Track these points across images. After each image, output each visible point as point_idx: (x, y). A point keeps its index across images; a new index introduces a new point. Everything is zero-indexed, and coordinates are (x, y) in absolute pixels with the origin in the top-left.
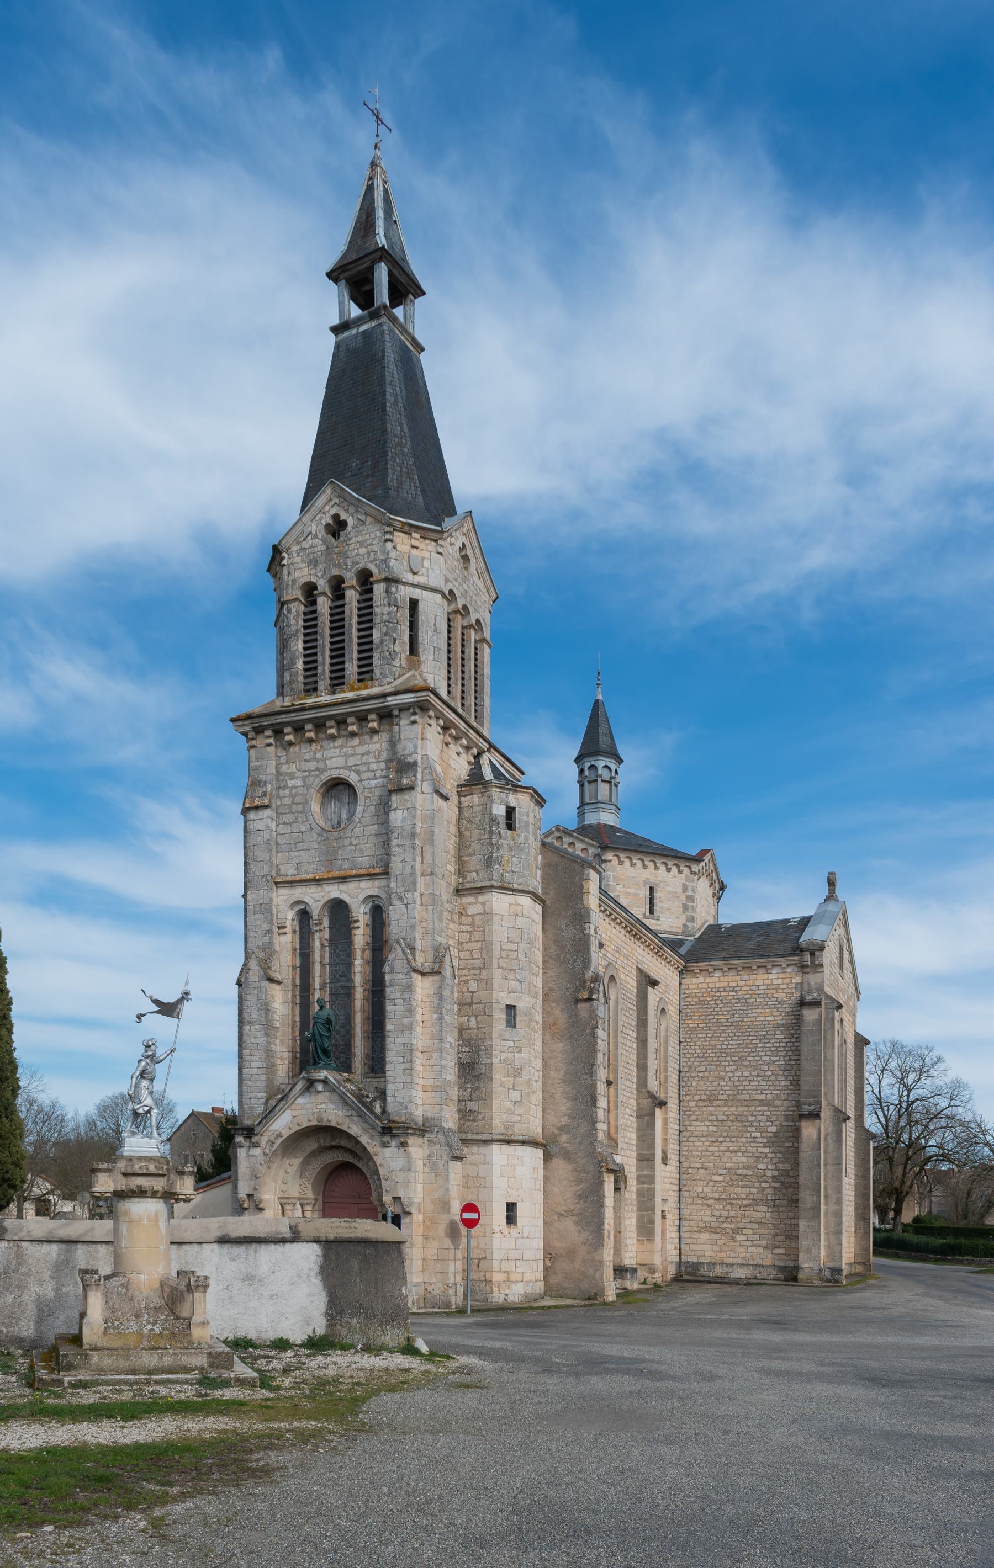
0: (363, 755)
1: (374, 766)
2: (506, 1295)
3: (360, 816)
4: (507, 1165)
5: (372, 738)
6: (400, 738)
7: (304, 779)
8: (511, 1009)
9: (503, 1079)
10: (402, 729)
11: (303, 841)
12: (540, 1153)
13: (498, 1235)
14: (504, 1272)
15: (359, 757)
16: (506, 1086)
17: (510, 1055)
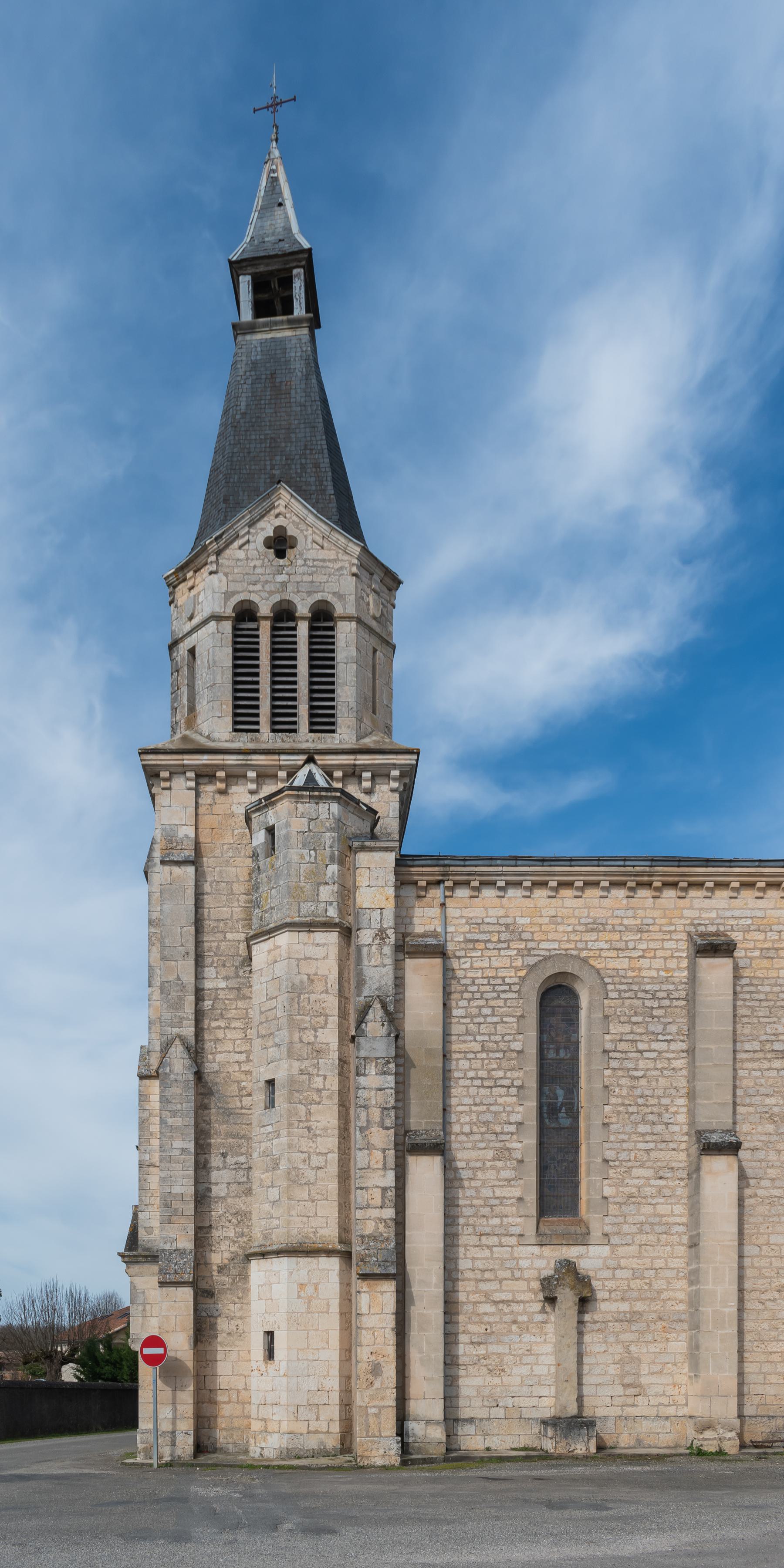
2: (262, 1448)
4: (264, 1284)
8: (271, 1083)
9: (263, 1176)
12: (333, 1264)
13: (256, 1373)
14: (262, 1420)
16: (265, 1184)
17: (269, 1144)
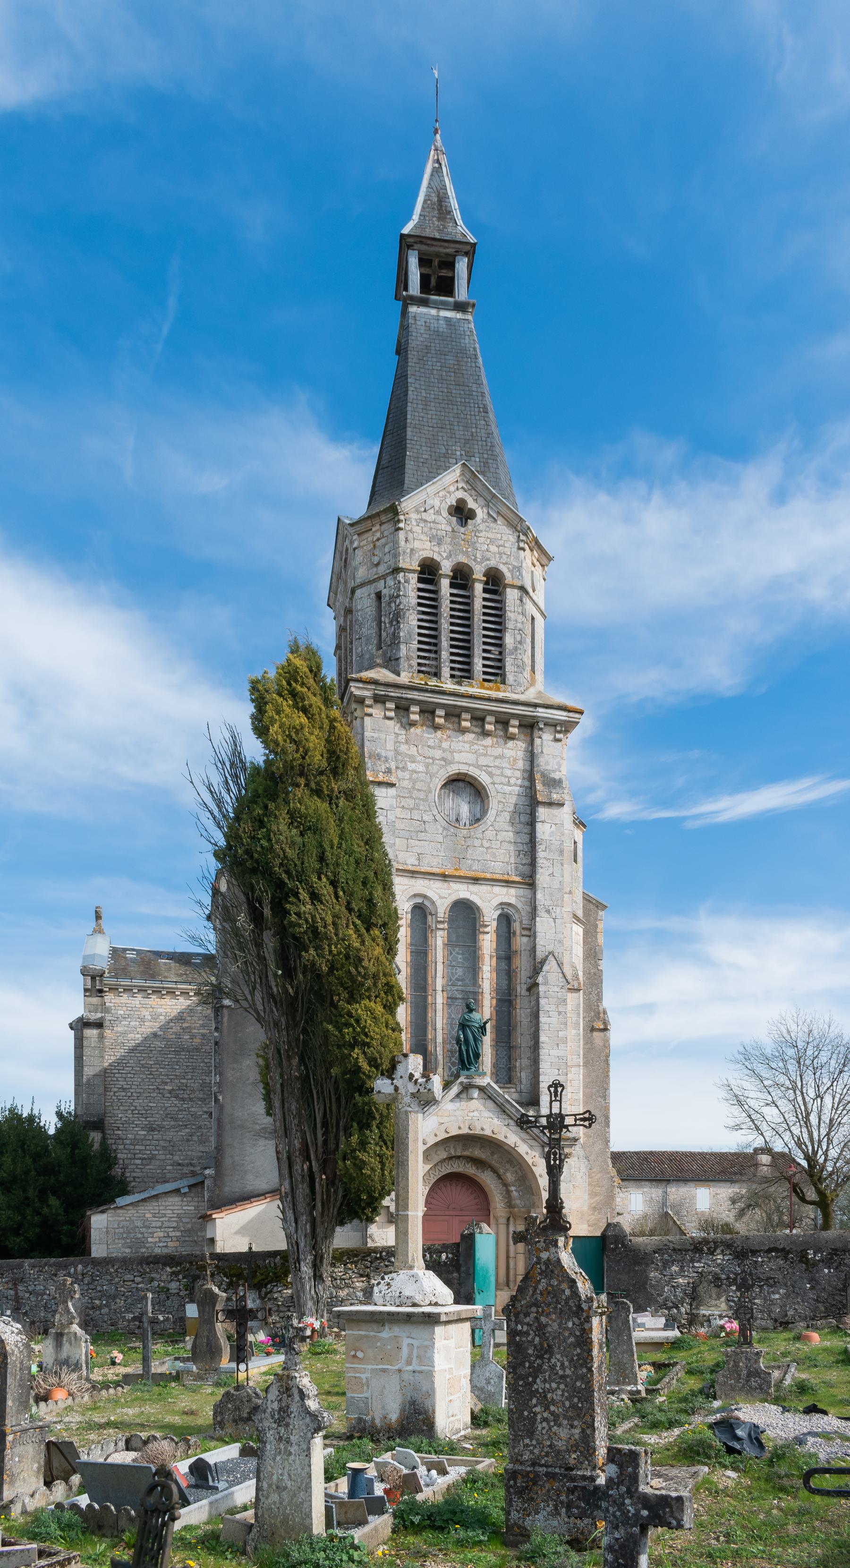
0: (496, 757)
1: (508, 773)
3: (493, 819)
5: (506, 743)
6: (542, 752)
7: (427, 766)
10: (545, 743)
11: (425, 831)
15: (492, 758)
